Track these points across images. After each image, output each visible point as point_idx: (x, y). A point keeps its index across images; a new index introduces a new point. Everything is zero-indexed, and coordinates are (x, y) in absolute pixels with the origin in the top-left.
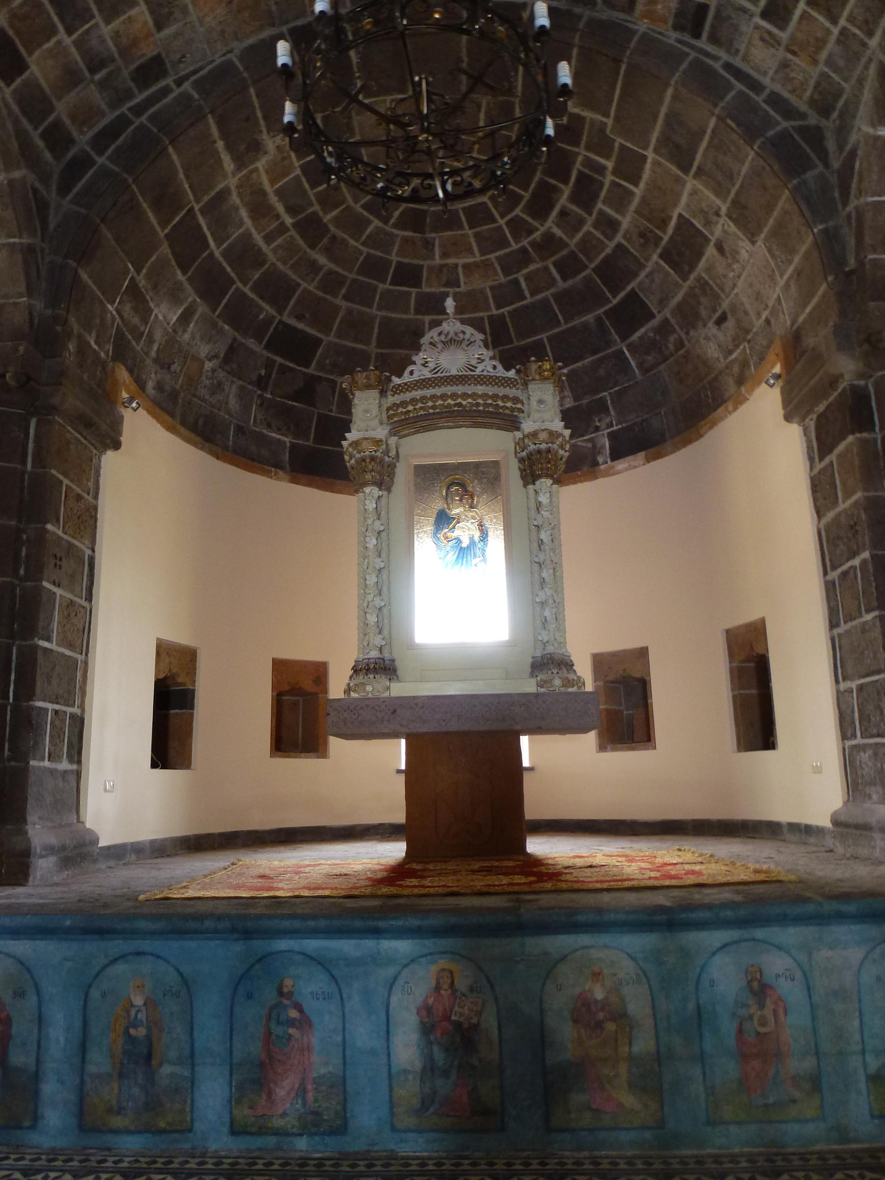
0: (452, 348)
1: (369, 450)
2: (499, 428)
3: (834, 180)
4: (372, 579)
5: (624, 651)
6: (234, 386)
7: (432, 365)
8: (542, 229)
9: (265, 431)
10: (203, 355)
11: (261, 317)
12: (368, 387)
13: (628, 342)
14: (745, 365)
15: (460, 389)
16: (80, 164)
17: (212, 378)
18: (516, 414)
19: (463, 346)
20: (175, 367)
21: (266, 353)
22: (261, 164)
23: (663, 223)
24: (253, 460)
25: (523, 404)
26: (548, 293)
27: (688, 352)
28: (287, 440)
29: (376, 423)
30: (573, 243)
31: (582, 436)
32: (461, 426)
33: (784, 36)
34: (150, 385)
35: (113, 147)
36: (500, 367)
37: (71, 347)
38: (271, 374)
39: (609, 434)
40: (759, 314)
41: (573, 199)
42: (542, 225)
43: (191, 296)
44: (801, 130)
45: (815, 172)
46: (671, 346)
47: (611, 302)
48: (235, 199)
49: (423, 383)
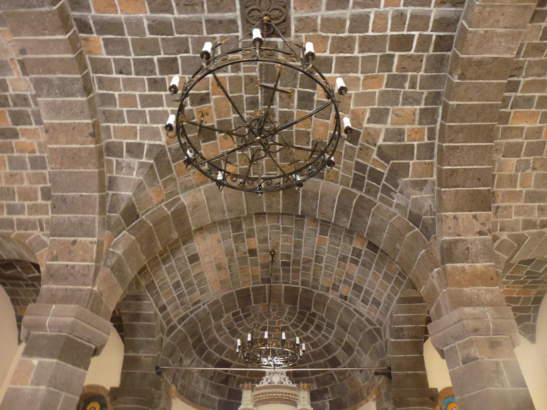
0: (276, 374)
2: (290, 405)
3: (384, 344)
7: (269, 381)
12: (248, 389)
14: (368, 387)
15: (278, 390)
16: (173, 328)
19: (280, 374)
22: (222, 320)
23: (342, 341)
24: (205, 406)
27: (352, 378)
28: (217, 398)
29: (249, 402)
30: (316, 339)
33: (368, 307)
34: (179, 385)
35: (183, 323)
36: (291, 383)
37: (163, 384)
41: (315, 328)
43: (195, 355)
44: (375, 329)
45: (379, 342)
46: (347, 375)
48: (213, 328)
49: (265, 387)
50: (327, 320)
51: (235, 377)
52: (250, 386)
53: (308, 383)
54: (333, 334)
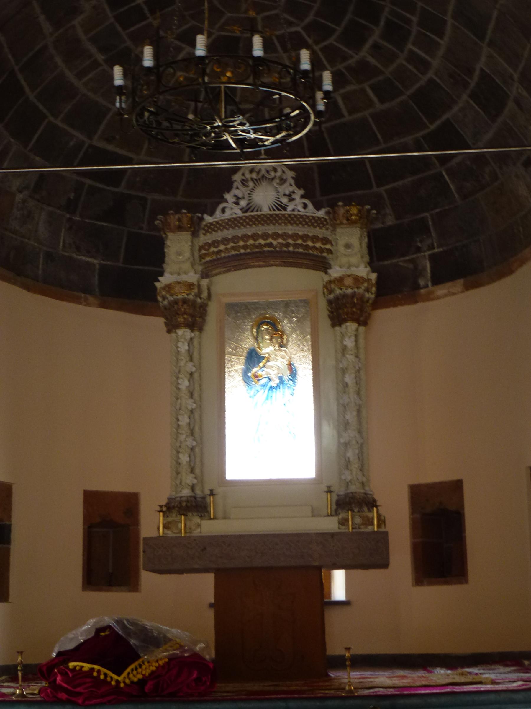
0: (264, 183)
1: (181, 294)
2: (308, 267)
4: (184, 420)
5: (441, 483)
7: (243, 203)
8: (357, 57)
9: (74, 255)
11: (72, 143)
12: (180, 228)
15: (271, 229)
18: (325, 254)
19: (275, 183)
22: (77, 21)
23: (470, 72)
25: (332, 245)
29: (187, 266)
31: (403, 255)
32: (271, 265)
36: (310, 206)
42: (357, 54)
49: (233, 223)
50: (420, 4)
52: (185, 220)
53: (360, 202)
54: (441, 52)
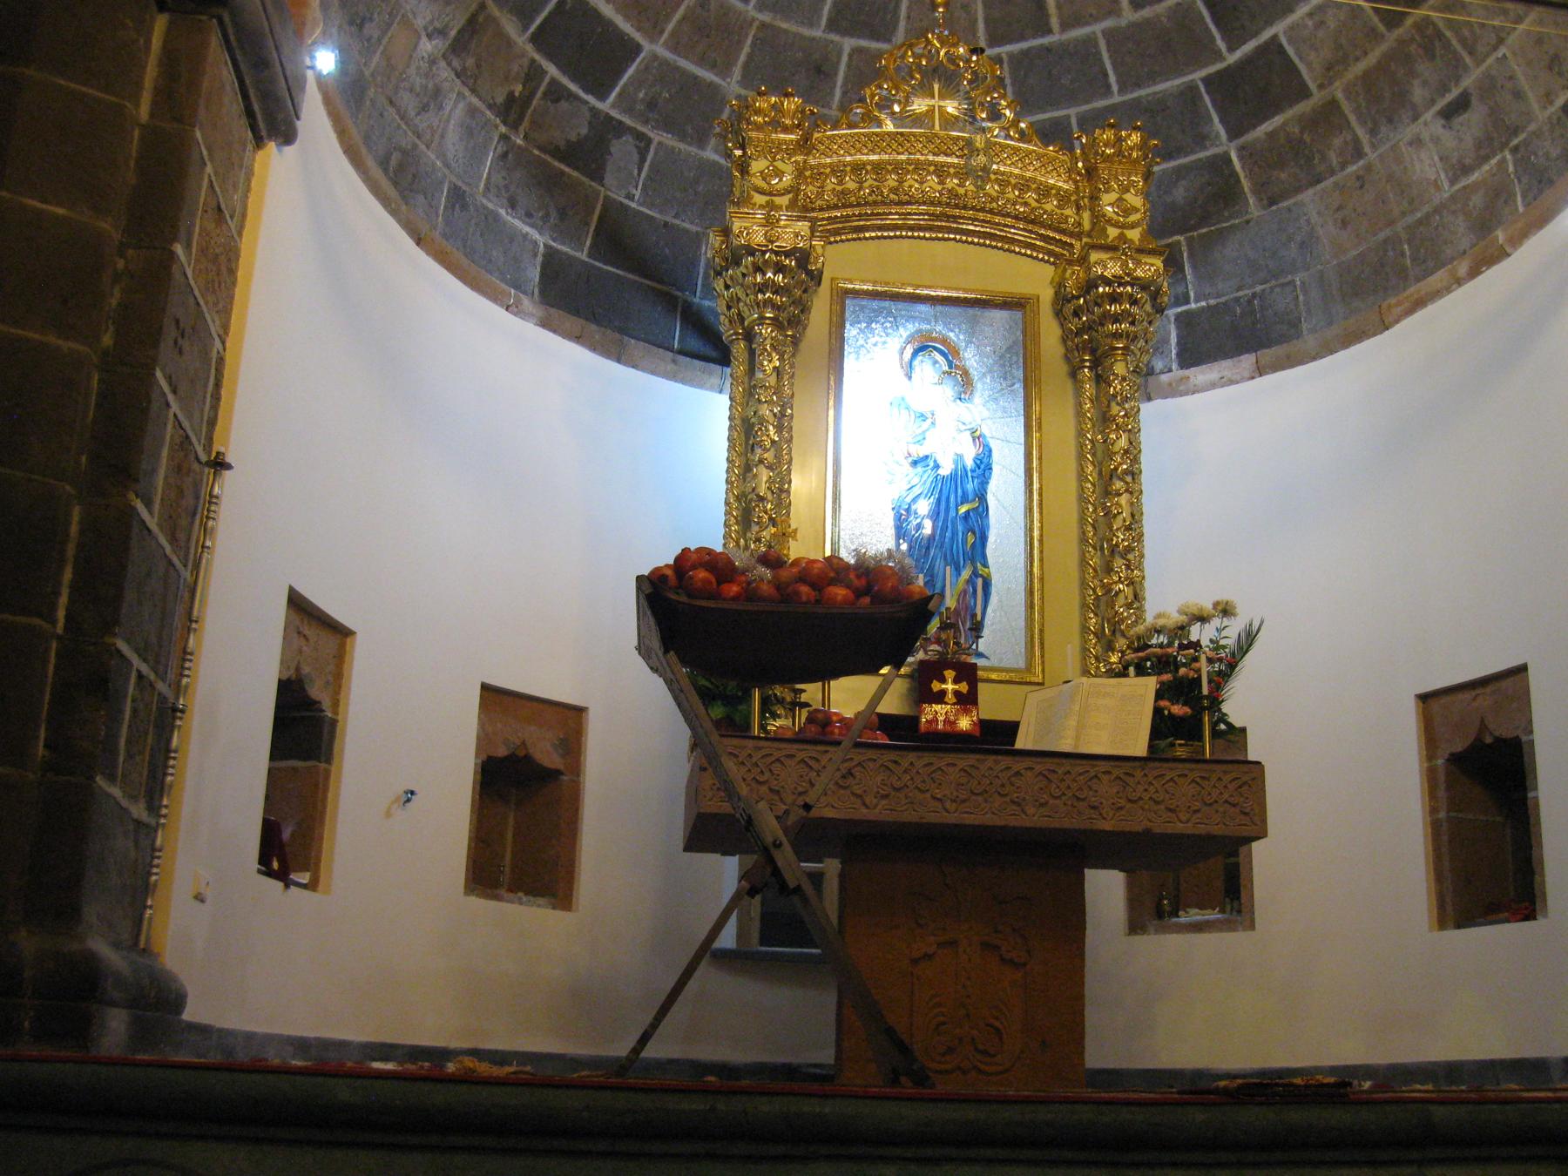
6: (461, 105)
9: (502, 212)
10: (420, 22)
13: (1241, 141)
14: (1499, 193)
17: (427, 75)
20: (371, 30)
21: (532, 52)
26: (1097, 28)
28: (541, 239)
38: (532, 94)
39: (1178, 317)
40: (1548, 98)
47: (1221, 58)
51: (643, 142)
